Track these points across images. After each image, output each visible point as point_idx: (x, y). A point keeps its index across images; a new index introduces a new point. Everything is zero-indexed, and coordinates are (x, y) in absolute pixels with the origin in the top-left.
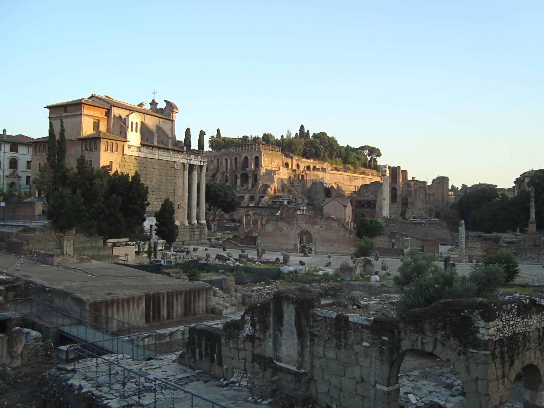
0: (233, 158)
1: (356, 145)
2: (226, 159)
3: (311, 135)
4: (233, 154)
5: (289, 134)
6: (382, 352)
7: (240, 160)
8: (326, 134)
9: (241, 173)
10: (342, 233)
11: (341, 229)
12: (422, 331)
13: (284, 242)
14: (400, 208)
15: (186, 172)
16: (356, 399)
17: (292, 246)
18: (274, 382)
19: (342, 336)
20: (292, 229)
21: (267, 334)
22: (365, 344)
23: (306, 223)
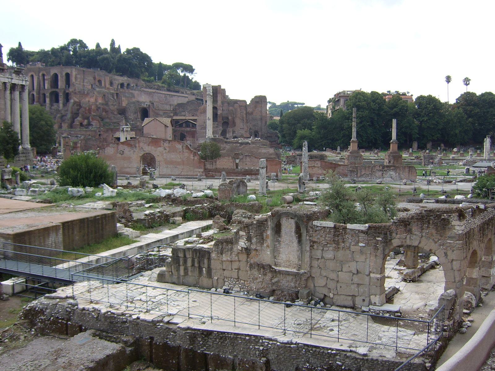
2: (32, 76)
4: (40, 70)
6: (376, 249)
9: (50, 91)
10: (186, 154)
12: (410, 231)
13: (125, 165)
14: (221, 128)
15: (8, 92)
16: (353, 287)
17: (135, 169)
18: (273, 284)
19: (341, 240)
20: (134, 151)
21: (265, 245)
22: (361, 244)
23: (149, 145)
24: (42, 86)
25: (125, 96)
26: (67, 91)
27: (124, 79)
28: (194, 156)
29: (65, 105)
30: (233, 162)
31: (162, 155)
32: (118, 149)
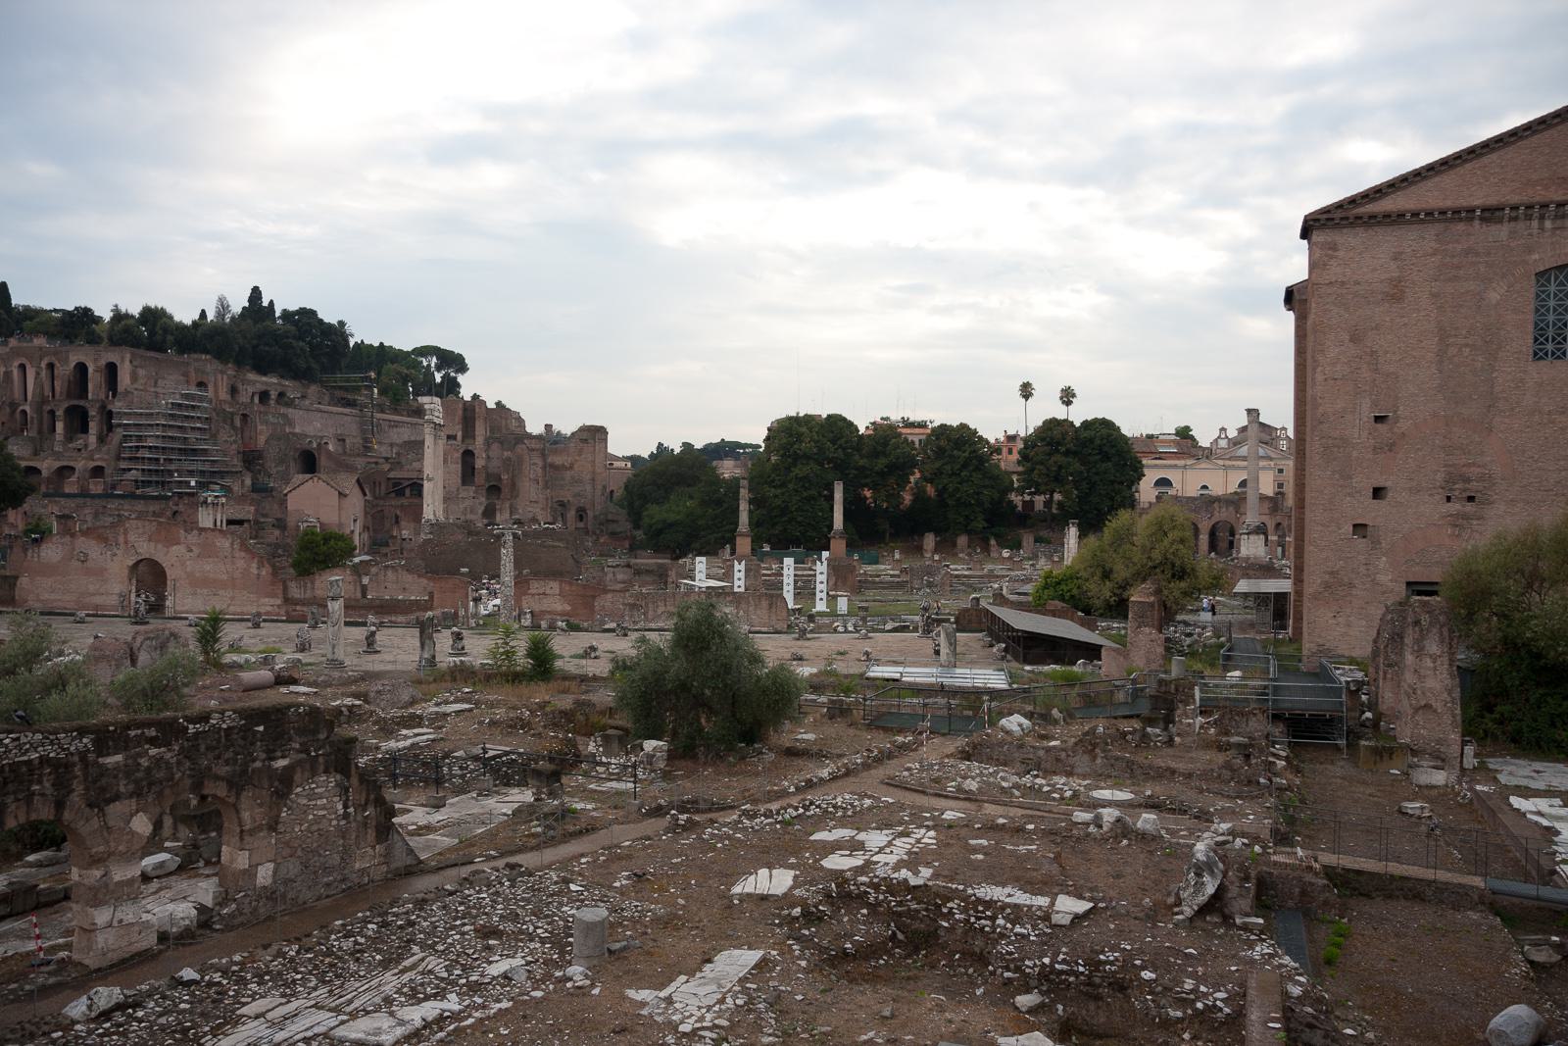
0: (43, 365)
1: (405, 343)
2: (22, 367)
3: (278, 314)
4: (42, 352)
5: (223, 306)
7: (65, 371)
8: (312, 313)
10: (241, 564)
11: (237, 555)
13: (92, 588)
14: (484, 499)
17: (116, 597)
20: (115, 555)
24: (48, 392)
25: (266, 423)
26: (110, 407)
27: (271, 380)
28: (258, 568)
29: (101, 439)
30: (355, 583)
31: (183, 564)
32: (74, 549)
